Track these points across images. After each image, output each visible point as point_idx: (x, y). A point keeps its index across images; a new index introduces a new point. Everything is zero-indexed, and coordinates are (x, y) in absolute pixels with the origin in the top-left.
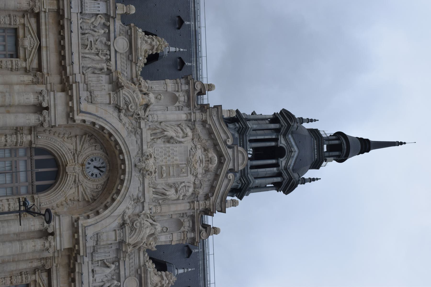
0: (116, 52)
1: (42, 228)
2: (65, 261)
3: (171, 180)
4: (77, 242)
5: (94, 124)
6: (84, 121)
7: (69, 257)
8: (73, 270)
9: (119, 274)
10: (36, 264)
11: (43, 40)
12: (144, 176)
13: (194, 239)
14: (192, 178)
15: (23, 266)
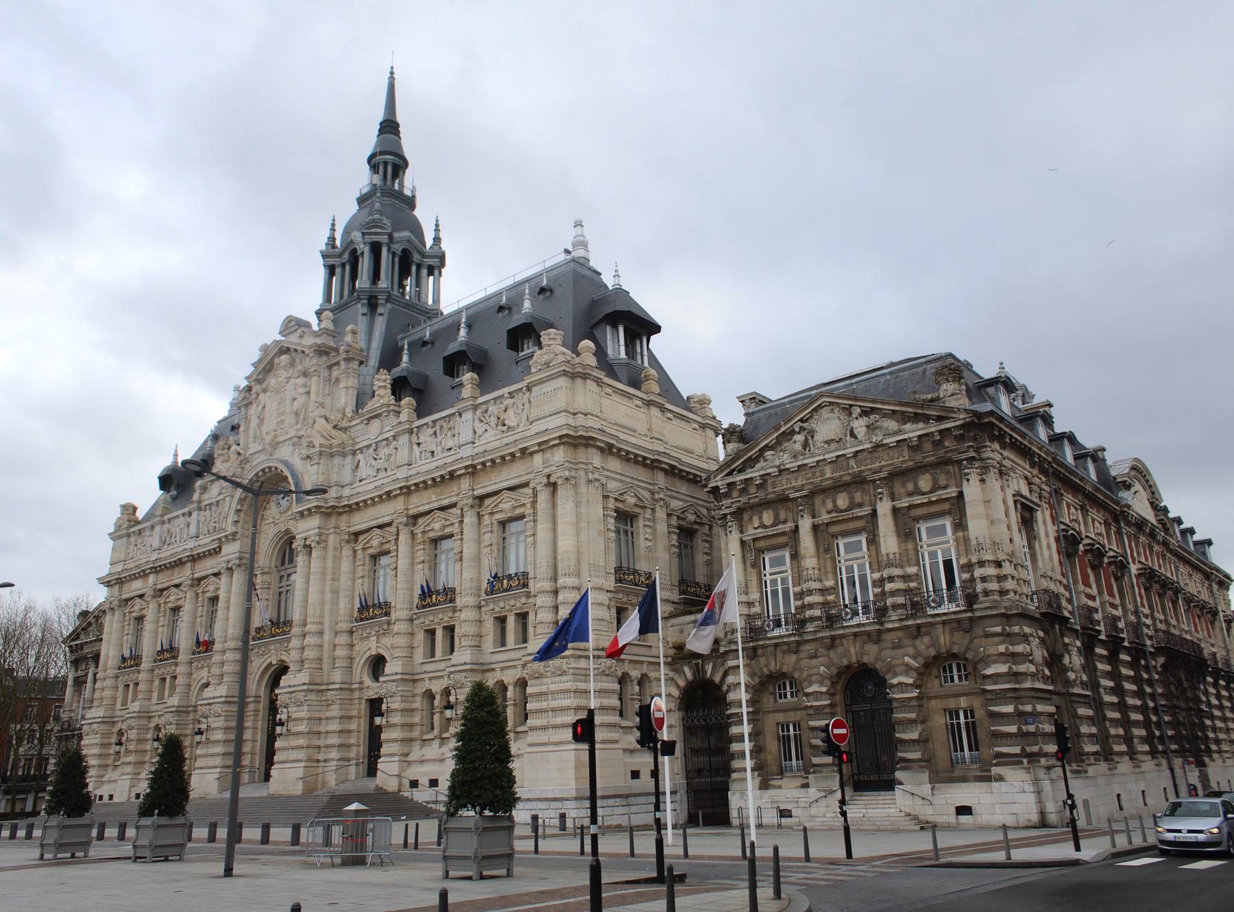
0: (220, 494)
1: (305, 551)
2: (344, 517)
3: (288, 409)
4: (309, 510)
5: (238, 511)
6: (237, 522)
7: (340, 514)
8: (349, 506)
9: (368, 446)
10: (347, 552)
11: (210, 572)
12: (278, 443)
13: (347, 360)
14: (292, 380)
15: (346, 566)
